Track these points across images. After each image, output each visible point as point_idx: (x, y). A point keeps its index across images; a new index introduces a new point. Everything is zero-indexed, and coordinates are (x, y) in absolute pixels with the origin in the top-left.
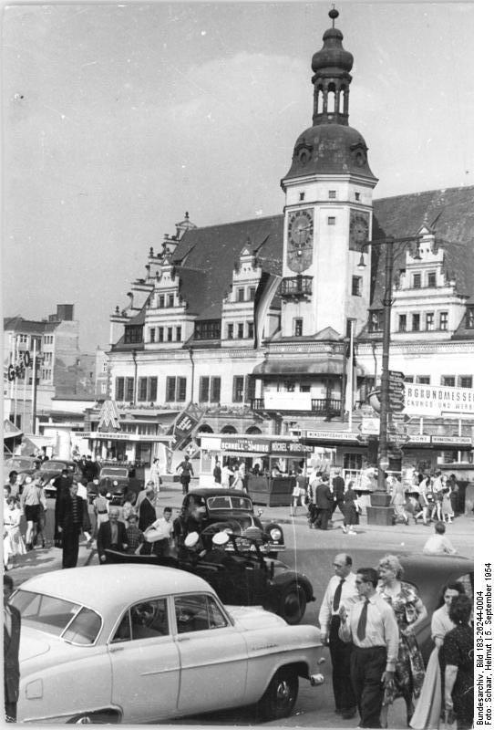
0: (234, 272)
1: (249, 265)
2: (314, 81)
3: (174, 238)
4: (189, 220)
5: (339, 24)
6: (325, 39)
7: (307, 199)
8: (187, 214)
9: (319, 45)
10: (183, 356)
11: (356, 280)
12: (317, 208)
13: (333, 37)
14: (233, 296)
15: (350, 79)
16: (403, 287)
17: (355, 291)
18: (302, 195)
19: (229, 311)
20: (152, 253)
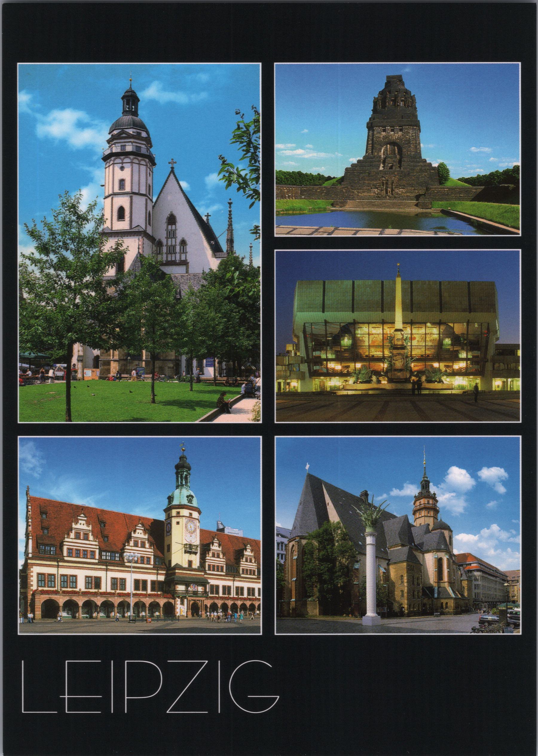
0: (132, 533)
1: (141, 531)
6: (180, 458)
19: (128, 549)
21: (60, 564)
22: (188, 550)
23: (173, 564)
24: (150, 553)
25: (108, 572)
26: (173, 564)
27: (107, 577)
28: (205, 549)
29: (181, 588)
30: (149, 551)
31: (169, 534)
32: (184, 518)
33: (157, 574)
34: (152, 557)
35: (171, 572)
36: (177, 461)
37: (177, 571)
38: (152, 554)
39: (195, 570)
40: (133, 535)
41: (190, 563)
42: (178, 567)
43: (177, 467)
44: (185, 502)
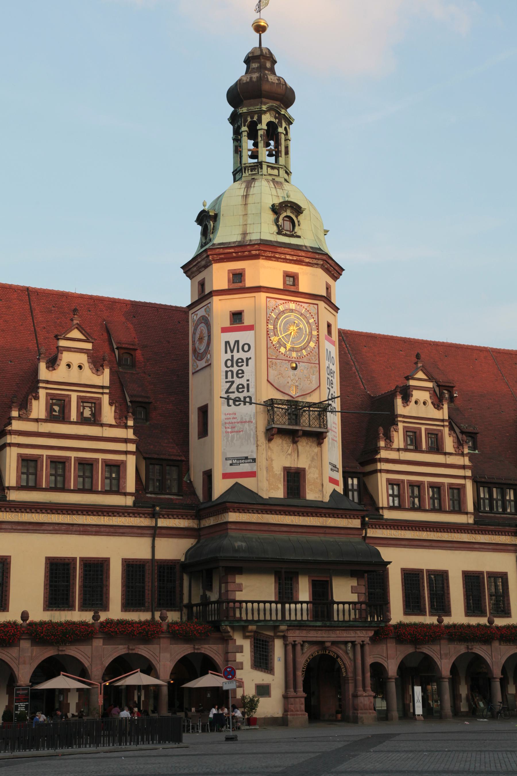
1: (83, 358)
13: (260, 60)
22: (282, 422)
23: (220, 487)
24: (121, 447)
26: (220, 487)
28: (369, 421)
29: (255, 590)
30: (114, 439)
31: (202, 364)
32: (263, 296)
33: (155, 532)
34: (131, 462)
35: (211, 521)
36: (238, 71)
37: (233, 517)
38: (132, 447)
39: (316, 509)
40: (44, 373)
41: (294, 479)
42: (242, 498)
43: (235, 96)
44: (266, 230)
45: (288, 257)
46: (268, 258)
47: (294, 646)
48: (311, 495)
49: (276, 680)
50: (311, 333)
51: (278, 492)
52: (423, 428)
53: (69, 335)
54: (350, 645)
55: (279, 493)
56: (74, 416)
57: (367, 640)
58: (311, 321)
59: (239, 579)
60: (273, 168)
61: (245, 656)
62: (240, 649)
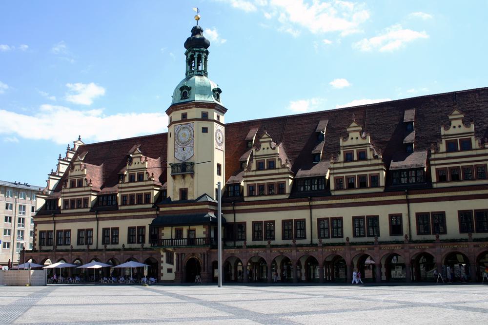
2: (186, 54)
3: (72, 150)
4: (81, 140)
5: (201, 25)
7: (189, 117)
8: (80, 136)
9: (190, 35)
10: (91, 216)
11: (219, 166)
12: (196, 122)
13: (196, 31)
14: (127, 179)
15: (207, 53)
16: (252, 169)
17: (219, 173)
18: (184, 116)
20: (60, 157)
21: (57, 218)
25: (100, 222)
27: (97, 227)
32: (173, 125)
41: (184, 193)
45: (182, 108)
46: (176, 110)
47: (178, 255)
48: (189, 198)
49: (174, 267)
50: (191, 134)
51: (178, 199)
52: (266, 159)
53: (135, 153)
54: (200, 255)
55: (178, 199)
56: (136, 180)
57: (205, 252)
58: (191, 129)
59: (163, 232)
60: (191, 72)
61: (164, 259)
62: (162, 256)
